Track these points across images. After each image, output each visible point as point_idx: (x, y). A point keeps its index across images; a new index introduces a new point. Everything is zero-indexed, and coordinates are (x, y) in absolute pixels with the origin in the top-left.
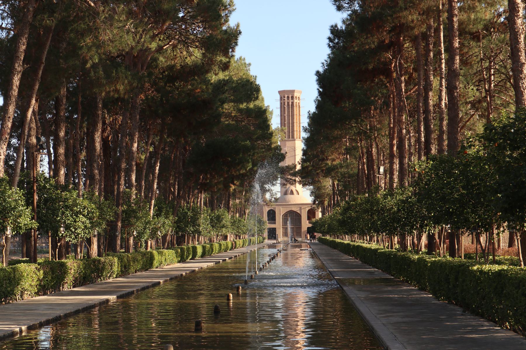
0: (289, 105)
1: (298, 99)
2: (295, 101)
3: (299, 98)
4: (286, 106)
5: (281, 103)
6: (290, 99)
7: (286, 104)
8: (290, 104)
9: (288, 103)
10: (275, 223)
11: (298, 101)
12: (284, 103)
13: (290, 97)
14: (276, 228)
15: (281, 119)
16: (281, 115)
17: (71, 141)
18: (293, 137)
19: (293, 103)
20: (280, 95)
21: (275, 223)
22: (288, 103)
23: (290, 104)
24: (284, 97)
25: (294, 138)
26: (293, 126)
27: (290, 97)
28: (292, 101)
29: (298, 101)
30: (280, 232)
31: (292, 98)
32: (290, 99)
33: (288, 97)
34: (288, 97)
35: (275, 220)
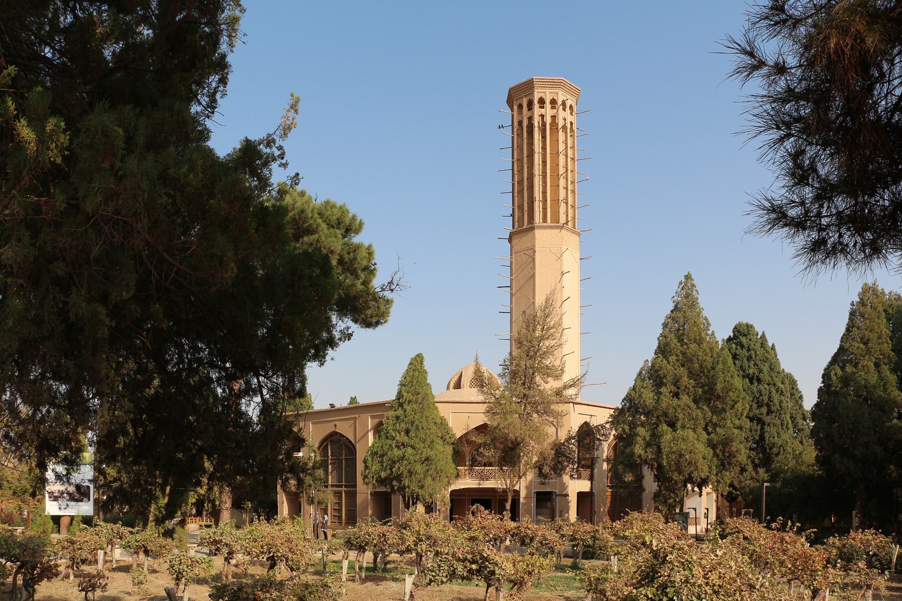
0: (544, 124)
1: (568, 109)
2: (562, 114)
3: (571, 107)
4: (536, 124)
5: (520, 123)
6: (548, 105)
7: (536, 121)
8: (548, 120)
11: (570, 118)
12: (530, 119)
19: (554, 117)
23: (548, 120)
29: (570, 118)
31: (553, 102)
32: (548, 105)
33: (542, 101)
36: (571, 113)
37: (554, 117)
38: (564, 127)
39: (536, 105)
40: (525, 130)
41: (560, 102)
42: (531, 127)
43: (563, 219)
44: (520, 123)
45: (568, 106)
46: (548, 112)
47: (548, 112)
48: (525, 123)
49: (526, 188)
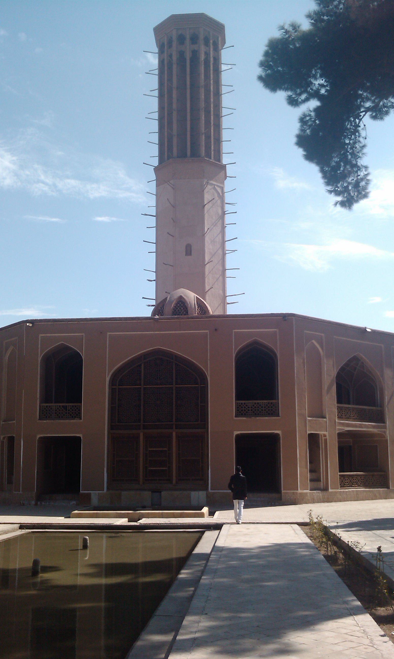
0: (184, 60)
2: (203, 49)
5: (161, 63)
6: (188, 42)
8: (188, 56)
9: (182, 55)
10: (77, 414)
12: (171, 56)
13: (188, 37)
18: (195, 154)
19: (195, 54)
21: (77, 414)
22: (182, 55)
23: (188, 56)
25: (199, 156)
26: (195, 120)
27: (188, 37)
28: (195, 47)
31: (194, 39)
32: (188, 42)
34: (181, 39)
38: (207, 62)
39: (174, 44)
40: (166, 68)
41: (201, 37)
42: (170, 65)
45: (211, 41)
48: (166, 62)
49: (166, 124)
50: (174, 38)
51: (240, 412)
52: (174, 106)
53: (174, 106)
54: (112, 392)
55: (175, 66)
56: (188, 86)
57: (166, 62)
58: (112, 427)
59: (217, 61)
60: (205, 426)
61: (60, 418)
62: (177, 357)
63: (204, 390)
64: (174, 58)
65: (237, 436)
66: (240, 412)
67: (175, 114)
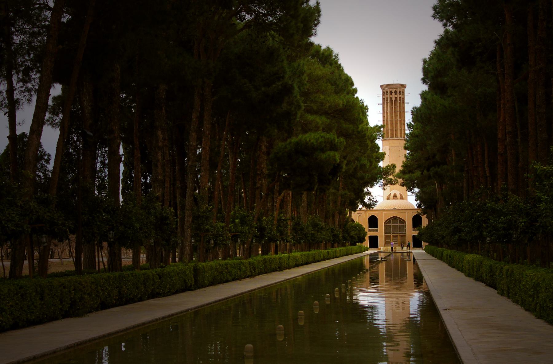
3: (403, 92)
4: (389, 101)
5: (383, 99)
6: (393, 93)
8: (394, 99)
9: (391, 98)
10: (377, 231)
12: (387, 98)
13: (393, 92)
14: (378, 236)
15: (384, 117)
16: (383, 112)
17: (98, 144)
19: (396, 98)
20: (383, 90)
21: (377, 231)
22: (391, 98)
23: (394, 99)
24: (387, 92)
26: (396, 124)
27: (393, 92)
28: (396, 96)
30: (381, 241)
31: (396, 92)
32: (393, 93)
34: (391, 92)
35: (376, 226)
36: (403, 95)
37: (396, 98)
43: (399, 136)
44: (384, 98)
46: (394, 96)
47: (394, 96)
50: (389, 92)
51: (413, 230)
52: (389, 119)
53: (389, 119)
54: (385, 225)
55: (389, 104)
56: (394, 111)
57: (385, 100)
58: (385, 234)
59: (403, 98)
60: (406, 233)
61: (373, 231)
62: (399, 218)
63: (405, 225)
64: (389, 99)
65: (413, 236)
66: (413, 230)
67: (389, 121)
